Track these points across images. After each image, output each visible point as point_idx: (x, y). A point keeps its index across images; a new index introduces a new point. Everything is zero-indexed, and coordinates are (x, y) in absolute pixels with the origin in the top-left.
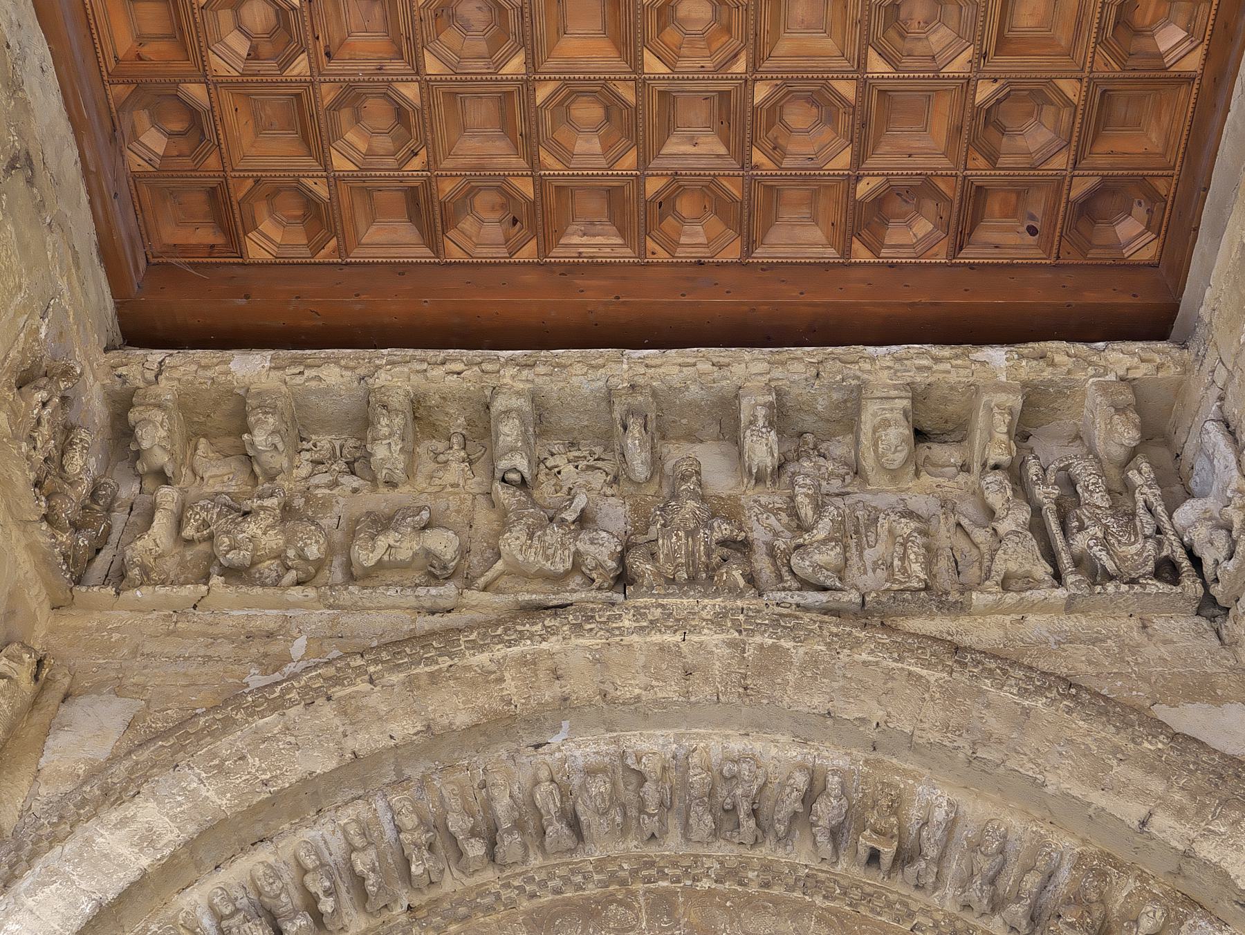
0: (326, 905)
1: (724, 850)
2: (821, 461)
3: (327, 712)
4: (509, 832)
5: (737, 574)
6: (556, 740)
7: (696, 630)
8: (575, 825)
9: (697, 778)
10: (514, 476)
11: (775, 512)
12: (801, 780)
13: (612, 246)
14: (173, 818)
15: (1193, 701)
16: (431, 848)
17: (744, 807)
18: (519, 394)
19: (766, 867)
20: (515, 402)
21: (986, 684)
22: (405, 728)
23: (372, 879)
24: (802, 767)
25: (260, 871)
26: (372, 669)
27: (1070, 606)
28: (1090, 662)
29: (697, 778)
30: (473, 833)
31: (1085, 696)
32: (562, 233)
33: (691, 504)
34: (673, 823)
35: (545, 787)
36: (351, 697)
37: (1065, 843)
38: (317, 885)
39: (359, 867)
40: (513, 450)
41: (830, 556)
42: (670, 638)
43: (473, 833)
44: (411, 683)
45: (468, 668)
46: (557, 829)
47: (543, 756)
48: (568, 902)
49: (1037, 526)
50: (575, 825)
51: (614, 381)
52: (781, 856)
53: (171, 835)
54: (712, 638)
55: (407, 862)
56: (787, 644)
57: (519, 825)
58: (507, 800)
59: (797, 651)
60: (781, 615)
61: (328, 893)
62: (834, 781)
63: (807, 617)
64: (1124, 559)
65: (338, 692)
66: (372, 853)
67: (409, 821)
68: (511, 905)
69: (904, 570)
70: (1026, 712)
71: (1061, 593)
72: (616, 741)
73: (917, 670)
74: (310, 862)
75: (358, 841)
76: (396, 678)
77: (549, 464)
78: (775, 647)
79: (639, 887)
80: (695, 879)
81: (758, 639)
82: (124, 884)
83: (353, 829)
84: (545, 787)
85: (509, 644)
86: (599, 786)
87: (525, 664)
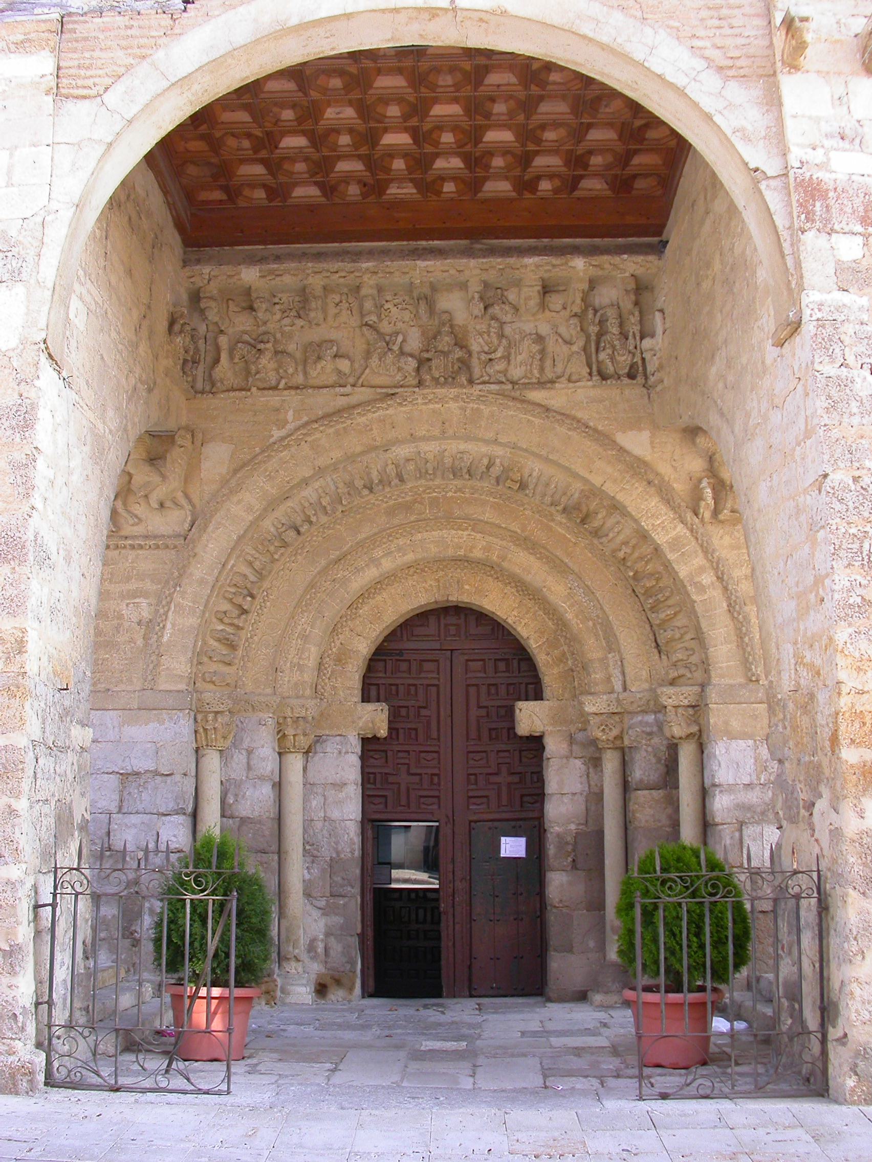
0: (314, 519)
1: (458, 483)
2: (503, 306)
3: (305, 447)
4: (377, 485)
5: (464, 379)
6: (393, 449)
7: (447, 402)
8: (402, 480)
9: (448, 461)
10: (371, 322)
11: (481, 334)
12: (485, 461)
13: (411, 194)
14: (257, 499)
15: (632, 430)
16: (349, 494)
17: (465, 470)
18: (371, 287)
19: (472, 488)
20: (370, 291)
21: (556, 426)
22: (337, 454)
23: (328, 508)
24: (485, 455)
25: (289, 510)
26: (321, 428)
27: (594, 386)
28: (598, 413)
29: (448, 461)
30: (365, 487)
31: (591, 432)
32: (387, 188)
33: (447, 339)
34: (439, 473)
35: (390, 467)
36: (314, 440)
37: (578, 486)
38: (310, 512)
39: (324, 503)
40: (370, 313)
41: (500, 366)
42: (436, 406)
43: (365, 487)
44: (337, 433)
45: (358, 424)
46: (396, 481)
47: (388, 455)
48: (400, 504)
49: (585, 349)
50: (402, 480)
51: (412, 280)
52: (478, 484)
53: (258, 506)
54: (453, 405)
55: (341, 498)
56: (482, 407)
57: (381, 481)
58: (376, 473)
59: (486, 410)
60: (481, 396)
61: (314, 515)
62: (498, 461)
63: (491, 396)
64: (618, 363)
65: (309, 439)
66: (328, 498)
67: (341, 485)
68: (379, 505)
69: (531, 370)
70: (569, 438)
71: (590, 383)
72: (416, 447)
73: (530, 418)
74: (307, 504)
75: (323, 495)
76: (332, 430)
77: (386, 307)
78: (478, 409)
79: (426, 496)
80: (447, 492)
81: (471, 405)
82: (245, 527)
83: (320, 491)
84: (390, 467)
85: (374, 412)
86: (411, 467)
87: (380, 421)
